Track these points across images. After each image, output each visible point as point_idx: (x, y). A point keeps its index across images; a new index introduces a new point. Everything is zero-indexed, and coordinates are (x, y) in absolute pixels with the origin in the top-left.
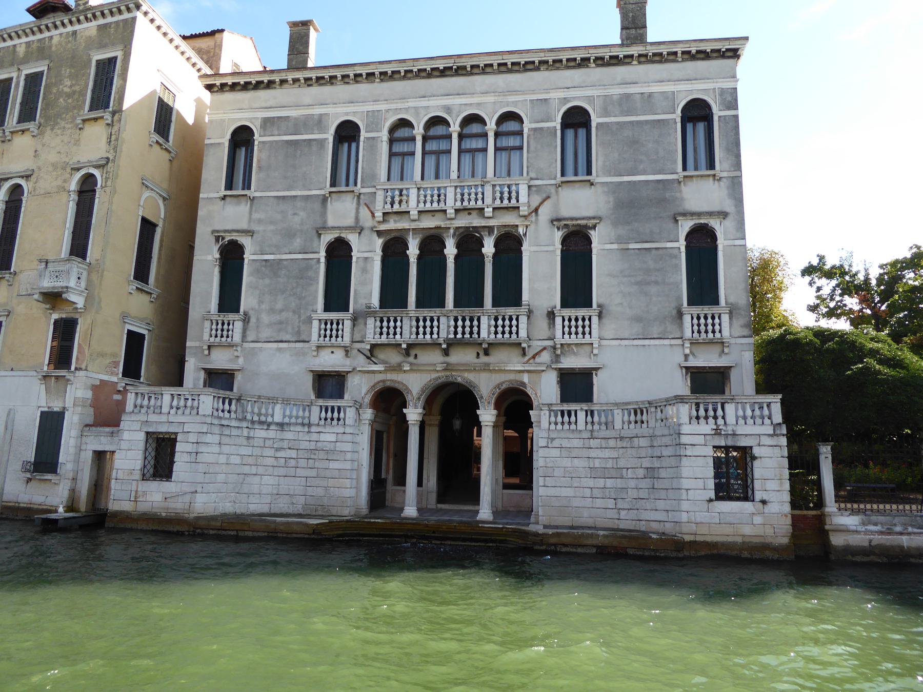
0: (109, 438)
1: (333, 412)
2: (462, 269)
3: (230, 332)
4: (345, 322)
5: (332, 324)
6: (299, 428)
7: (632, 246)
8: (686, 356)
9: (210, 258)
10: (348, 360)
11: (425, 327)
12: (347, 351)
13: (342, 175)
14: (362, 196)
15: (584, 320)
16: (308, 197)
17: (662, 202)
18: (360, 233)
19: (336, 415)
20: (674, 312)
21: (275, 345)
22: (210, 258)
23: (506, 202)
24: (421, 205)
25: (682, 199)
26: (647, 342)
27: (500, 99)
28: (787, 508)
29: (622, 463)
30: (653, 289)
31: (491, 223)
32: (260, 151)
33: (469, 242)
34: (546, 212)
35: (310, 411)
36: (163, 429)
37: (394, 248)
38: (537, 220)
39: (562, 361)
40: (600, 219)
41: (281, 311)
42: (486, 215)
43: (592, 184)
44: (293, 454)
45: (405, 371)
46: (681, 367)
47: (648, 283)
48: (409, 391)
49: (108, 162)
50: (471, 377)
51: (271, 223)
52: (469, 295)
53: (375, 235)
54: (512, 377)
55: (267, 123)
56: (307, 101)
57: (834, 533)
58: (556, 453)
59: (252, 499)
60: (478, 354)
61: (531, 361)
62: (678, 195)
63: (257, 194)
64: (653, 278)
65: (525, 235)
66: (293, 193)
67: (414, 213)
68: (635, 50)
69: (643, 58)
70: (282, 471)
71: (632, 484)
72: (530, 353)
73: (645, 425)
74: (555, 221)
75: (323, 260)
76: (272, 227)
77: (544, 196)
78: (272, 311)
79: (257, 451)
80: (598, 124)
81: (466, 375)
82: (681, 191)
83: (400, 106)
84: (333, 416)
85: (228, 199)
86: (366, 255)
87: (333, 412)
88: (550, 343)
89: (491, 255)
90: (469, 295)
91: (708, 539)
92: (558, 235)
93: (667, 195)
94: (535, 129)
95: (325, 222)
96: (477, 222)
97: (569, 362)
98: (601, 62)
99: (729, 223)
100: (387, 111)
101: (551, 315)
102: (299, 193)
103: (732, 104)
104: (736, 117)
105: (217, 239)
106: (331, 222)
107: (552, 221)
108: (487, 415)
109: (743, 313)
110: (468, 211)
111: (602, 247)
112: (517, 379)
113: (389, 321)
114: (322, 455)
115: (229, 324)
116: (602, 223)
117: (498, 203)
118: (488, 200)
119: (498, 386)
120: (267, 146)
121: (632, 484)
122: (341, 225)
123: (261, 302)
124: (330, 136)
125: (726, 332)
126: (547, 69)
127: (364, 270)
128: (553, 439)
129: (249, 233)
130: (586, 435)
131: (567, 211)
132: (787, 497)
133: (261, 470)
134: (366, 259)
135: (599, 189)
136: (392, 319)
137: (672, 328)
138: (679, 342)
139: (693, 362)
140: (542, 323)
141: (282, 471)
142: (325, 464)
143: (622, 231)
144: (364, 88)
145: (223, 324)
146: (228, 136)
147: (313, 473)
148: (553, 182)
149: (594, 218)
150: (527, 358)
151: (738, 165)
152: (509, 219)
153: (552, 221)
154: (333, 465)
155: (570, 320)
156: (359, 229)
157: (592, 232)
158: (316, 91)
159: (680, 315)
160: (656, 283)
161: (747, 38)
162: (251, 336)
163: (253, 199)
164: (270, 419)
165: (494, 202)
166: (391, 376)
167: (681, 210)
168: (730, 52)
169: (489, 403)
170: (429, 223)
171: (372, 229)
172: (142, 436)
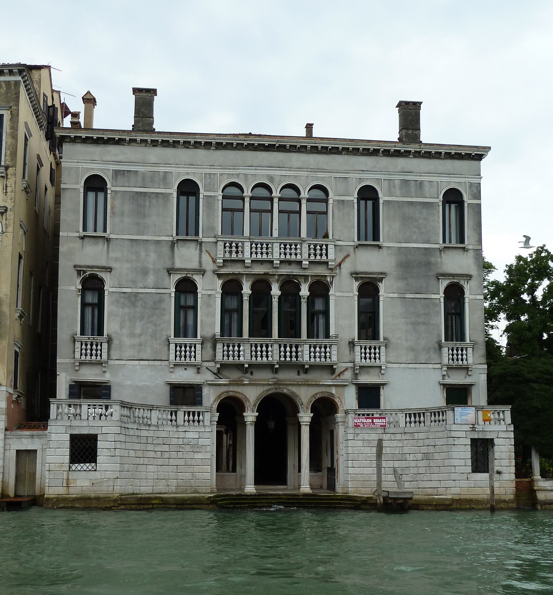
0: (30, 440)
1: (194, 416)
2: (277, 306)
3: (99, 352)
4: (197, 345)
5: (185, 347)
6: (170, 428)
7: (408, 296)
8: (444, 376)
9: (73, 288)
10: (199, 375)
11: (262, 352)
12: (199, 369)
13: (188, 227)
14: (203, 244)
15: (375, 349)
16: (158, 242)
17: (428, 265)
18: (203, 275)
19: (196, 417)
20: (437, 345)
21: (137, 363)
22: (73, 288)
23: (318, 257)
24: (254, 256)
25: (442, 263)
26: (417, 366)
27: (312, 174)
28: (513, 477)
29: (406, 450)
30: (422, 328)
31: (307, 273)
32: (113, 199)
33: (290, 286)
34: (347, 268)
35: (176, 416)
36: (85, 431)
37: (231, 288)
38: (340, 272)
39: (359, 378)
40: (384, 274)
41: (140, 335)
42: (303, 266)
43: (380, 247)
44: (166, 448)
45: (244, 385)
46: (440, 384)
47: (419, 324)
48: (247, 400)
49: (6, 210)
50: (294, 389)
51: (128, 261)
52: (290, 329)
53: (216, 276)
54: (323, 389)
55: (117, 173)
56: (153, 159)
57: (540, 492)
58: (360, 443)
59: (143, 483)
60: (299, 372)
61: (338, 378)
62: (439, 260)
63: (112, 236)
64: (422, 320)
65: (332, 283)
66: (145, 238)
67: (248, 261)
68: (412, 148)
69: (418, 154)
70: (160, 462)
71: (413, 464)
72: (337, 372)
73: (422, 424)
74: (355, 275)
75: (173, 295)
76: (127, 265)
77: (346, 254)
78: (132, 335)
79: (143, 447)
80: (385, 201)
81: (290, 388)
82: (441, 257)
83: (232, 172)
84: (195, 419)
85: (86, 240)
86: (209, 292)
87: (194, 416)
88: (351, 365)
89: (306, 297)
90: (290, 329)
91: (468, 497)
92: (356, 285)
93: (433, 260)
94: (339, 201)
95: (173, 263)
96: (295, 270)
97: (365, 379)
98: (387, 153)
99: (473, 283)
100: (221, 174)
101: (352, 344)
102: (150, 238)
103: (478, 196)
104: (479, 205)
105: (79, 272)
106: (178, 264)
107: (352, 274)
108: (305, 417)
109: (481, 347)
110: (289, 262)
111: (386, 295)
112: (327, 391)
113: (234, 346)
114: (188, 448)
115: (97, 345)
116: (387, 278)
117: (312, 258)
118: (306, 256)
119: (314, 396)
120: (119, 194)
121: (413, 464)
122: (188, 267)
123: (122, 327)
124: (173, 191)
125: (470, 360)
126: (347, 154)
127: (208, 305)
128: (358, 434)
129: (109, 269)
130: (383, 431)
131: (361, 268)
132: (513, 469)
133: (146, 461)
134: (210, 295)
135: (384, 251)
136: (236, 345)
137: (434, 356)
138: (439, 366)
139: (448, 381)
140: (346, 350)
141: (160, 462)
142: (191, 455)
143: (401, 284)
144: (201, 153)
145: (92, 345)
146: (83, 184)
147: (182, 462)
148: (352, 244)
149: (382, 273)
150: (334, 376)
151: (480, 241)
152: (320, 271)
153: (352, 274)
154: (199, 456)
155: (365, 349)
156: (202, 272)
157: (380, 284)
158: (160, 151)
159: (440, 347)
160: (424, 323)
161: (490, 148)
162: (115, 354)
163: (108, 240)
164: (149, 423)
165: (309, 257)
166: (232, 388)
167: (441, 271)
168: (476, 155)
169: (307, 408)
170: (259, 270)
171: (214, 272)
172: (67, 437)
